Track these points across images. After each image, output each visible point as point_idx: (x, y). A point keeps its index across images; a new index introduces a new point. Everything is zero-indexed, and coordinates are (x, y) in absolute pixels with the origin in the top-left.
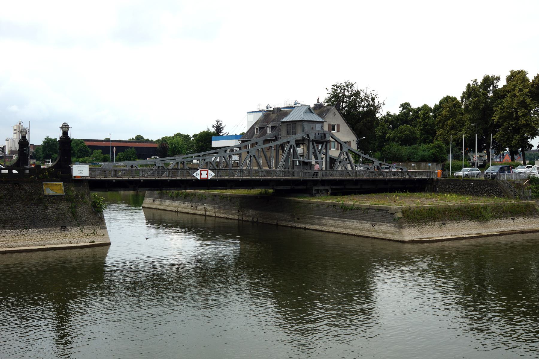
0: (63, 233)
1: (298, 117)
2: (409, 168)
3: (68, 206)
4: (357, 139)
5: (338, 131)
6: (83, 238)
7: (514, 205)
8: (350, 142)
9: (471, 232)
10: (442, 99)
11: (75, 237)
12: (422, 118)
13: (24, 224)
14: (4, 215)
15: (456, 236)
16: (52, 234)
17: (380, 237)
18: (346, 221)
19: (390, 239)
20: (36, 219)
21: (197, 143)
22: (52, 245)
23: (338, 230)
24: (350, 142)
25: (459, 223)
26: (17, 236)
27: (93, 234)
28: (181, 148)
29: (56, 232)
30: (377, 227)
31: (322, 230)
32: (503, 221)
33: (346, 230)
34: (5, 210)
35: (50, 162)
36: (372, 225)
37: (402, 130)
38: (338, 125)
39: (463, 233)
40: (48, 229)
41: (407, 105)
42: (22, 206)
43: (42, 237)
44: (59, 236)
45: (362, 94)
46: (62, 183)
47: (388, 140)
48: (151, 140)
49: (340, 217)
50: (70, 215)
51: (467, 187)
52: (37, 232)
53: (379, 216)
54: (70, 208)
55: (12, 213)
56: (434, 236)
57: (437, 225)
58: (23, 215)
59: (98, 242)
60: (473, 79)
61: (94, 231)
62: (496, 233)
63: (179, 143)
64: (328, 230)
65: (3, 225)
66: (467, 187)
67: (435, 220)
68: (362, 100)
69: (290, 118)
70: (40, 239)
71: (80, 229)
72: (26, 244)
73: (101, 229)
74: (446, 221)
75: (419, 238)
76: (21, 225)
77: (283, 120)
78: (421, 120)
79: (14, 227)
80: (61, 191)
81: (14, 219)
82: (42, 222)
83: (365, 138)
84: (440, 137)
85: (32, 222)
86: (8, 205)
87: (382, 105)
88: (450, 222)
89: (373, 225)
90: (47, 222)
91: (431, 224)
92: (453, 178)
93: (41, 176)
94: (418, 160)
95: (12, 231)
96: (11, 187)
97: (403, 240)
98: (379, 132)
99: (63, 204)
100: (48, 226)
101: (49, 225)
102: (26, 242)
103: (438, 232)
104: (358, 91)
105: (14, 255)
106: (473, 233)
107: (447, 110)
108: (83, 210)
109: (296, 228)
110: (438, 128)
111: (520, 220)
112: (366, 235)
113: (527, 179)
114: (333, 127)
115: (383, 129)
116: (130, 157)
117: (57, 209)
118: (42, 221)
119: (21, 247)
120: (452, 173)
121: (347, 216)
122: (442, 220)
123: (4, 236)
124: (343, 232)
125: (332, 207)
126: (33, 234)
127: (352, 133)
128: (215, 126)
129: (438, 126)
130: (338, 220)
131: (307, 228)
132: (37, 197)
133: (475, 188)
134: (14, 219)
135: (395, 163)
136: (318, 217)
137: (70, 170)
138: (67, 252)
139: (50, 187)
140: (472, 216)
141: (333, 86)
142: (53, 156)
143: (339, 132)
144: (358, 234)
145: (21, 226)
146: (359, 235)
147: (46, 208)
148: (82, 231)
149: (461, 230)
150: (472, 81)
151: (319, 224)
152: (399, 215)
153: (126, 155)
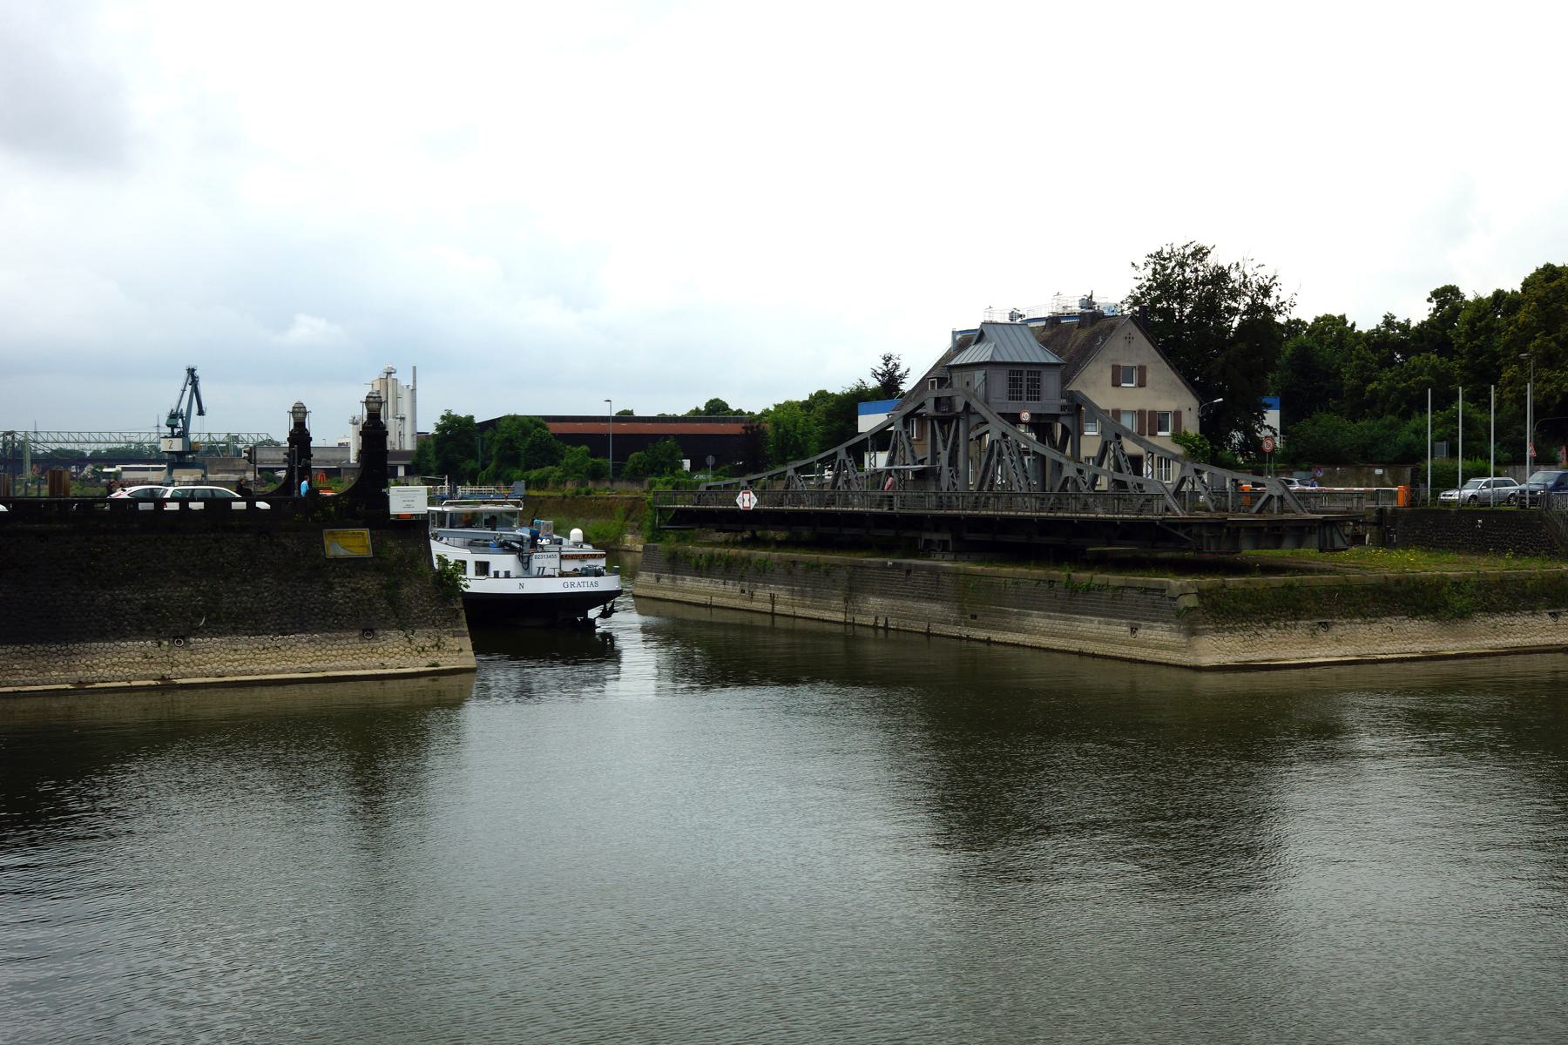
0: (366, 645)
1: (974, 356)
2: (1365, 481)
5: (1142, 384)
6: (411, 658)
7: (1562, 576)
8: (1177, 414)
9: (1408, 648)
10: (1533, 276)
12: (1466, 332)
13: (278, 624)
14: (235, 603)
15: (1358, 656)
16: (342, 647)
17: (1148, 659)
18: (1076, 620)
19: (1170, 662)
22: (341, 670)
23: (1058, 644)
24: (1177, 414)
25: (1372, 625)
26: (264, 649)
28: (803, 434)
29: (350, 641)
30: (1141, 633)
32: (1518, 621)
34: (238, 593)
35: (446, 481)
36: (1132, 629)
37: (1414, 368)
38: (1140, 367)
39: (1384, 648)
40: (333, 635)
41: (1452, 294)
42: (275, 583)
43: (319, 654)
44: (358, 652)
45: (1234, 275)
46: (366, 532)
49: (1063, 610)
53: (1146, 606)
54: (384, 587)
55: (254, 598)
56: (1289, 655)
57: (1301, 630)
58: (279, 603)
59: (447, 665)
61: (439, 640)
63: (796, 422)
64: (1037, 645)
65: (233, 624)
67: (1298, 616)
68: (1234, 294)
69: (974, 356)
70: (315, 658)
73: (454, 636)
74: (1332, 616)
75: (1242, 659)
77: (952, 363)
78: (1462, 341)
83: (1221, 400)
84: (1508, 389)
85: (297, 619)
87: (1287, 305)
88: (1345, 621)
89: (1134, 630)
90: (331, 620)
91: (1285, 625)
92: (1435, 508)
95: (253, 638)
97: (1198, 664)
99: (369, 578)
101: (335, 626)
103: (1304, 645)
104: (1222, 268)
105: (257, 690)
106: (1417, 649)
107: (1531, 308)
108: (415, 592)
109: (968, 639)
110: (1506, 364)
112: (1119, 655)
114: (1119, 376)
116: (663, 464)
117: (353, 590)
118: (320, 617)
119: (271, 674)
120: (1435, 494)
122: (1319, 616)
123: (235, 650)
124: (1071, 649)
125: (1047, 586)
126: (300, 645)
127: (1186, 389)
131: (992, 639)
132: (309, 563)
133: (1488, 534)
135: (1319, 469)
136: (1015, 610)
137: (385, 500)
138: (375, 685)
139: (340, 540)
141: (1149, 259)
142: (463, 466)
143: (1145, 386)
144: (1100, 653)
145: (272, 627)
146: (1104, 653)
147: (331, 587)
148: (410, 641)
149: (1377, 641)
151: (1019, 630)
152: (1190, 601)
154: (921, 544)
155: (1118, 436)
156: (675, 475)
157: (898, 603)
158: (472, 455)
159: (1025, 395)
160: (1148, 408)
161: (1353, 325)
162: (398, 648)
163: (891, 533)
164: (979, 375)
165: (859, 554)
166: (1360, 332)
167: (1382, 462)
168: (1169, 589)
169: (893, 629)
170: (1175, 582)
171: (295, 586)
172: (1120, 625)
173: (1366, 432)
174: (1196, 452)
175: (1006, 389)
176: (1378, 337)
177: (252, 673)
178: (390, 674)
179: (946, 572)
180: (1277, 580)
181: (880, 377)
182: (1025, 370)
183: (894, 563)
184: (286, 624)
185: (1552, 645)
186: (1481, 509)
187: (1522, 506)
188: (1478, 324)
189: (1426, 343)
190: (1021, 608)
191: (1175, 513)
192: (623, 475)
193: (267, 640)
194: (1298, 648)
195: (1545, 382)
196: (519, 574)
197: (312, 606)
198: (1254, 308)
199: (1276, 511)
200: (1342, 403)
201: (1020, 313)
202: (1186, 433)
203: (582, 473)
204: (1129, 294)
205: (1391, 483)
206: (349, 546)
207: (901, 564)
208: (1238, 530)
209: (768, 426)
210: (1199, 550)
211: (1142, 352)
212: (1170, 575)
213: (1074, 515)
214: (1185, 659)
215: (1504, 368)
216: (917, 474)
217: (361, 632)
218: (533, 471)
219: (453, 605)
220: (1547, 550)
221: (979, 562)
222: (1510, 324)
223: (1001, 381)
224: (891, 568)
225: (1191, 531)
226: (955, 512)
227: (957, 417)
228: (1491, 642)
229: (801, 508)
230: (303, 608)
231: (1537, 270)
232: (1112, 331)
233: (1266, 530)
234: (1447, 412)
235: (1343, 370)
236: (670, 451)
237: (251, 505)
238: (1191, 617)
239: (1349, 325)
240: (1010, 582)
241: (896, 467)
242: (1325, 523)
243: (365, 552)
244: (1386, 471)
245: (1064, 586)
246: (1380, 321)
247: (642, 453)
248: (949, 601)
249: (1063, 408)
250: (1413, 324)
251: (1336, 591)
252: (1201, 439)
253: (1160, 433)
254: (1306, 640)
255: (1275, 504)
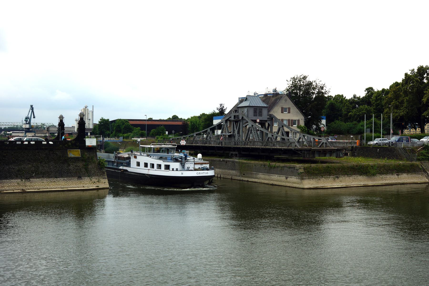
0: (79, 181)
3: (82, 164)
4: (305, 118)
5: (289, 112)
6: (91, 184)
7: (400, 164)
8: (299, 121)
10: (392, 85)
11: (86, 184)
12: (375, 100)
15: (346, 186)
17: (290, 186)
18: (271, 175)
19: (296, 187)
20: (62, 172)
21: (205, 122)
24: (299, 121)
25: (350, 177)
26: (51, 182)
27: (98, 182)
28: (198, 125)
29: (75, 180)
30: (289, 179)
31: (258, 182)
32: (388, 176)
33: (271, 181)
34: (44, 167)
36: (286, 178)
37: (361, 109)
38: (289, 108)
39: (353, 184)
41: (371, 89)
43: (66, 183)
44: (77, 183)
45: (314, 84)
46: (79, 150)
47: (350, 118)
48: (184, 119)
50: (84, 170)
51: (375, 153)
52: (63, 180)
53: (290, 172)
54: (84, 165)
57: (331, 178)
58: (55, 169)
60: (411, 68)
61: (99, 180)
62: (380, 184)
63: (197, 122)
65: (42, 175)
66: (375, 153)
67: (330, 175)
68: (314, 89)
71: (90, 179)
72: (56, 187)
73: (103, 179)
74: (339, 175)
75: (315, 186)
76: (54, 175)
77: (239, 106)
79: (49, 177)
80: (79, 155)
81: (49, 172)
82: (66, 174)
83: (310, 117)
84: (386, 115)
86: (46, 163)
87: (328, 92)
88: (343, 176)
89: (287, 178)
90: (69, 174)
91: (327, 177)
93: (66, 145)
94: (355, 133)
96: (48, 152)
97: (304, 187)
98: (345, 111)
100: (70, 176)
101: (70, 176)
102: (56, 186)
103: (332, 183)
104: (311, 82)
105: (49, 193)
106: (362, 184)
108: (92, 167)
109: (242, 180)
111: (405, 175)
112: (283, 185)
113: (422, 146)
114: (283, 110)
115: (348, 109)
116: (161, 133)
117: (75, 166)
118: (66, 173)
119: (52, 189)
120: (367, 143)
121: (271, 172)
122: (336, 175)
123: (43, 182)
126: (61, 181)
128: (219, 108)
129: (385, 106)
130: (267, 175)
133: (380, 153)
134: (49, 172)
136: (255, 173)
137: (85, 142)
139: (72, 153)
140: (362, 172)
141: (291, 79)
142: (106, 133)
144: (278, 184)
147: (69, 165)
148: (91, 180)
149: (351, 182)
150: (410, 70)
151: (256, 178)
152: (302, 171)
153: (157, 131)
154: (230, 155)
155: (283, 126)
156: (164, 136)
157: (224, 171)
158: (108, 129)
159: (258, 115)
160: (291, 119)
161: (345, 97)
162: (88, 182)
163: (222, 152)
164: (246, 110)
165: (213, 157)
166: (347, 99)
167: (353, 134)
168: (296, 167)
169: (222, 178)
170: (298, 166)
171: (59, 165)
172: (283, 177)
173: (349, 126)
174: (303, 131)
175: (253, 113)
176: (352, 100)
177: (47, 188)
178: (85, 189)
179: (237, 162)
180: (325, 165)
181: (219, 110)
182: (258, 108)
183: (223, 160)
184: (57, 175)
185: (397, 183)
186: (379, 146)
187: (389, 146)
188: (378, 97)
189: (364, 102)
190: (257, 172)
191: (298, 147)
192: (149, 135)
193: (51, 179)
194: (330, 183)
195: (395, 113)
196: (181, 170)
197: (64, 170)
198: (319, 93)
199: (324, 147)
200: (342, 118)
201: (257, 93)
202: (301, 126)
203: (138, 135)
204: (286, 88)
205: (355, 139)
206: (74, 154)
207: (224, 160)
208: (314, 151)
209: (189, 123)
210: (304, 157)
211: (289, 104)
212: (296, 163)
213: (271, 147)
214: (300, 186)
215: (385, 109)
216: (230, 136)
217: (78, 178)
218: (125, 134)
219: (103, 170)
220: (396, 158)
221: (246, 160)
222: (386, 98)
223: (251, 111)
224: (222, 161)
225: (302, 152)
226: (239, 146)
227: (240, 120)
228: (381, 182)
229: (198, 145)
230: (62, 171)
231: (393, 83)
232: (281, 98)
233: (322, 152)
234: (370, 121)
235: (342, 109)
236: (162, 129)
237: (48, 143)
238: (302, 175)
239: (344, 97)
240: (254, 165)
241: (223, 134)
242: (338, 150)
243: (79, 156)
244: (354, 136)
245: (268, 166)
246: (352, 96)
247: (154, 130)
248: (237, 170)
249: (268, 118)
250: (361, 97)
251: (340, 168)
252: (305, 127)
253: (294, 126)
254: (332, 181)
255: (324, 145)
